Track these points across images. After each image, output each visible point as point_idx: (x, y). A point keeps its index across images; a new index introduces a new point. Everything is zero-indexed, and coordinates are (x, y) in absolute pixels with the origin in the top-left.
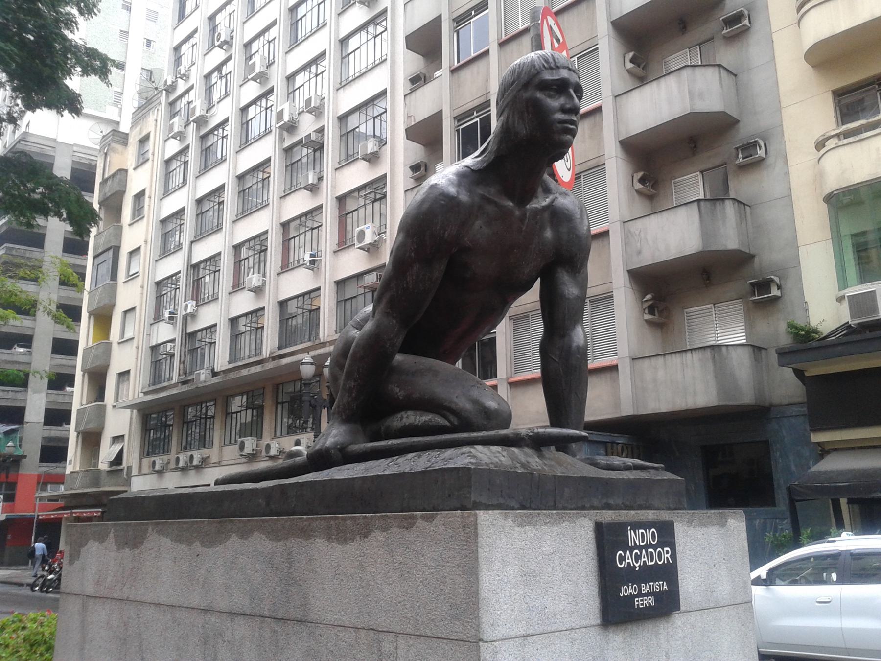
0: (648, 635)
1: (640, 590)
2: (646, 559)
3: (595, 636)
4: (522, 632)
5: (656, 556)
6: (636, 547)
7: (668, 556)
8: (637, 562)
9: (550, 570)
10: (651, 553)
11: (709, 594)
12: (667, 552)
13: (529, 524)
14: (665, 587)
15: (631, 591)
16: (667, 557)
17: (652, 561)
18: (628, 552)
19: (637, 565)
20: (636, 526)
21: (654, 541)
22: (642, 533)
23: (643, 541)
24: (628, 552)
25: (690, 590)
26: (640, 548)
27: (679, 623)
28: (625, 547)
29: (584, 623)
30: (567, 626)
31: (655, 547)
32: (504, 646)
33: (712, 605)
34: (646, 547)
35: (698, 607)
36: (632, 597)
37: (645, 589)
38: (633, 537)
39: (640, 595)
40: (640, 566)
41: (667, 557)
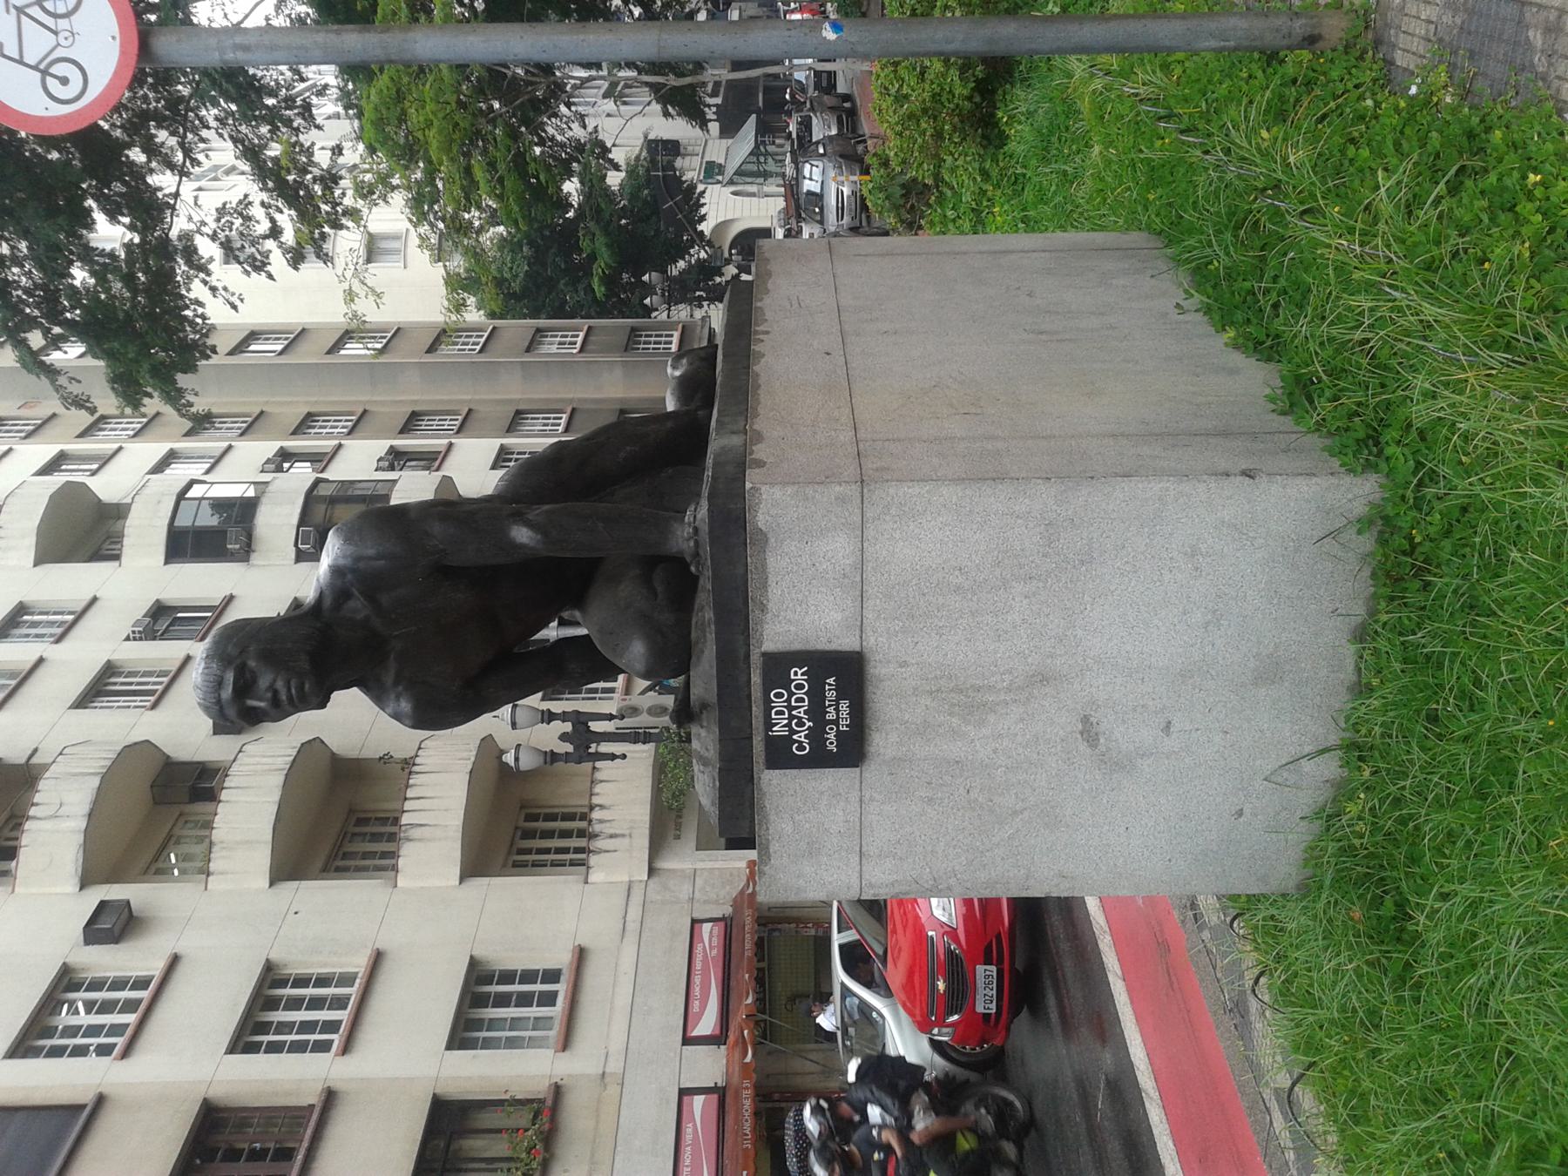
0: (879, 693)
1: (831, 722)
2: (802, 710)
3: (872, 770)
4: (857, 859)
5: (800, 694)
6: (789, 725)
7: (800, 672)
8: (804, 724)
9: (807, 825)
10: (796, 701)
11: (846, 580)
12: (796, 674)
13: (768, 848)
14: (831, 680)
15: (832, 736)
16: (802, 674)
17: (803, 701)
18: (795, 737)
19: (809, 724)
20: (769, 725)
21: (783, 695)
22: (776, 713)
23: (783, 713)
24: (795, 737)
25: (838, 616)
26: (791, 717)
27: (872, 640)
28: (788, 740)
29: (857, 786)
30: (857, 805)
31: (791, 694)
32: (866, 876)
33: (858, 579)
34: (791, 708)
35: (858, 603)
36: (839, 734)
37: (831, 716)
38: (778, 730)
39: (836, 722)
40: (809, 720)
41: (802, 674)
